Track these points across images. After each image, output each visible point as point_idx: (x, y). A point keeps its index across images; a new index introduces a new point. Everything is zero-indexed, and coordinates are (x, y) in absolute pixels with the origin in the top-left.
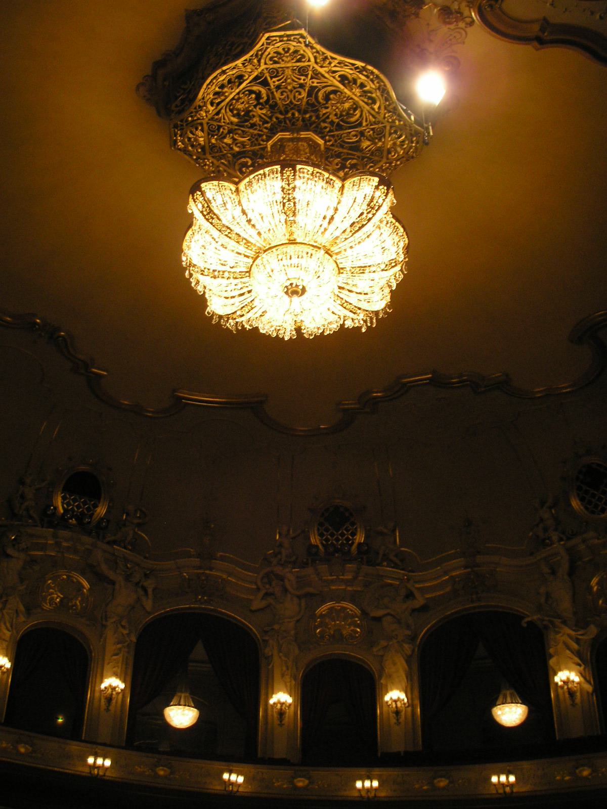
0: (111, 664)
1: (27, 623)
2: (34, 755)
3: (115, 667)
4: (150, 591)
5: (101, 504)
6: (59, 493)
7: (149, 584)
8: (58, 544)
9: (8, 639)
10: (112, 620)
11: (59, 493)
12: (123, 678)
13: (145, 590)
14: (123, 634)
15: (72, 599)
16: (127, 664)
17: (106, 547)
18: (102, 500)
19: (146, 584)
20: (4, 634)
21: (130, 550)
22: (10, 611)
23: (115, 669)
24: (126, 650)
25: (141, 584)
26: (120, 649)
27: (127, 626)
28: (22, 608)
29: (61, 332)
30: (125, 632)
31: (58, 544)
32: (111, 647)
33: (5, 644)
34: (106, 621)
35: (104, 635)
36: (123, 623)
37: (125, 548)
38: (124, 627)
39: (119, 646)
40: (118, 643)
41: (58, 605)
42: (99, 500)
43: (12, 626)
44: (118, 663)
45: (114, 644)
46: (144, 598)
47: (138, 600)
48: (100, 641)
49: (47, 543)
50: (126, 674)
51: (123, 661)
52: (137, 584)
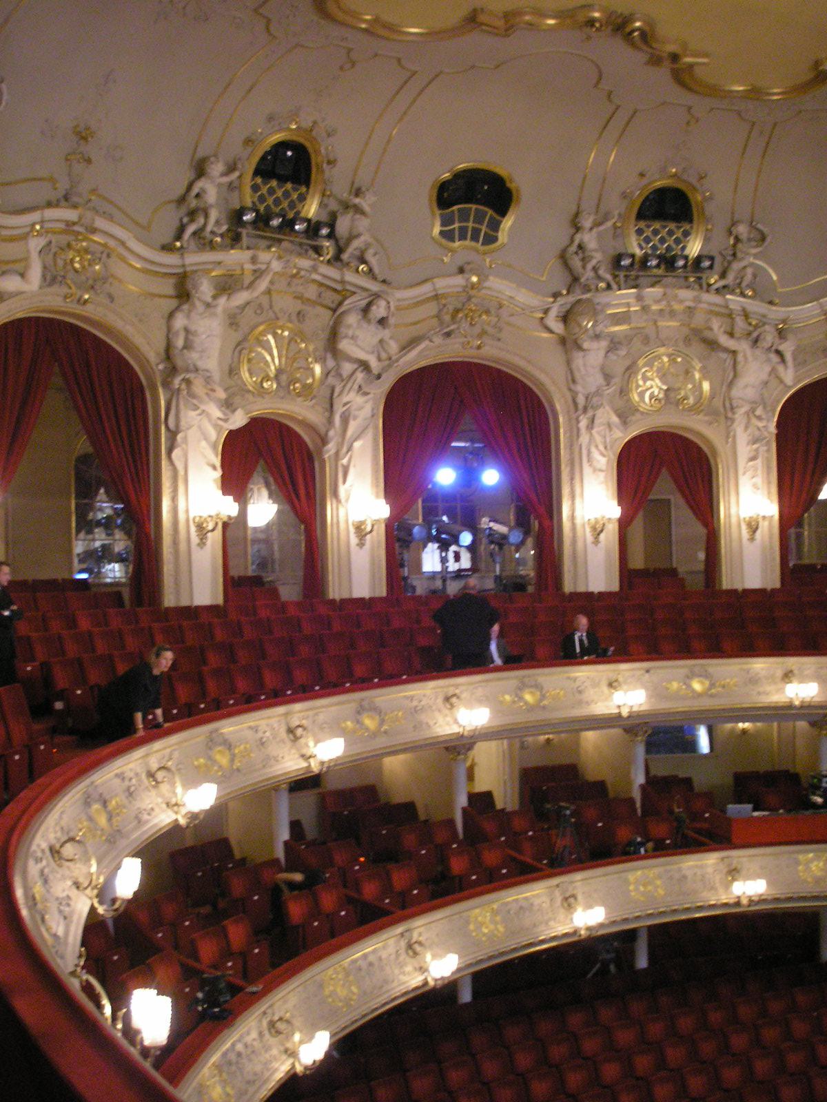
0: (748, 473)
1: (621, 437)
2: (713, 691)
3: (753, 477)
4: (788, 356)
5: (695, 226)
6: (631, 227)
7: (787, 348)
8: (645, 309)
9: (604, 468)
10: (743, 410)
11: (631, 226)
12: (766, 493)
13: (779, 353)
14: (759, 429)
15: (679, 389)
16: (769, 468)
17: (716, 299)
18: (695, 222)
19: (781, 348)
20: (598, 461)
21: (750, 297)
22: (602, 428)
23: (754, 480)
24: (765, 448)
25: (773, 348)
26: (757, 450)
27: (763, 417)
28: (615, 419)
29: (635, 22)
30: (760, 424)
31: (645, 309)
32: (744, 450)
33: (602, 475)
34: (734, 414)
35: (732, 434)
36: (758, 412)
37: (743, 295)
38: (759, 418)
39: (755, 446)
40: (755, 441)
41: (663, 402)
42: (691, 221)
43: (606, 448)
44: (756, 469)
45: (748, 444)
46: (781, 368)
47: (774, 370)
48: (727, 442)
49: (629, 311)
50: (769, 483)
51: (763, 466)
52: (769, 349)
